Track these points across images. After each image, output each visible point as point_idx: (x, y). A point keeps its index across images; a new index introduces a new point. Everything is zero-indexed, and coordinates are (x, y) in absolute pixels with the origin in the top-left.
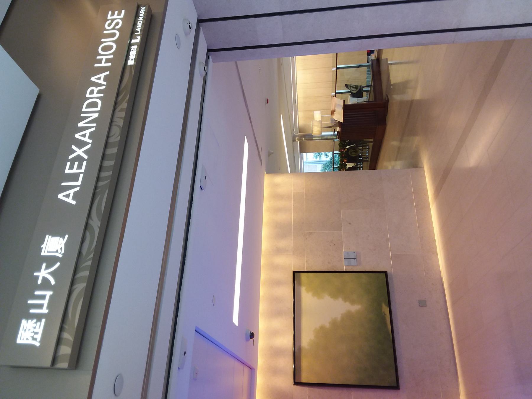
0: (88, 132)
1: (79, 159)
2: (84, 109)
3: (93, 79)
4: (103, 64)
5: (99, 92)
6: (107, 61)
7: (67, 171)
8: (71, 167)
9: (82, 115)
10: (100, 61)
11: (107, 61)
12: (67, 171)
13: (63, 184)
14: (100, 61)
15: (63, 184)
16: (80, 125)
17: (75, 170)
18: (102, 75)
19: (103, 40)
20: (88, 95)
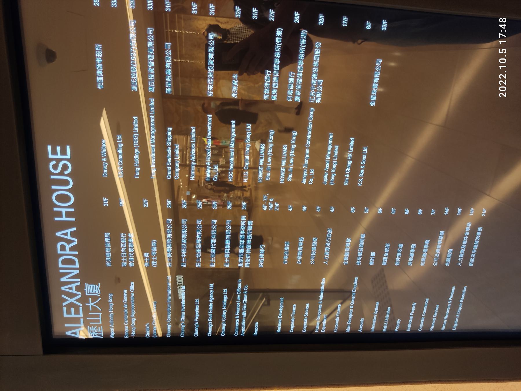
0: (73, 286)
1: (72, 305)
2: (61, 266)
3: (58, 234)
4: (64, 218)
5: (71, 249)
6: (68, 214)
7: (66, 315)
8: (69, 312)
9: (61, 271)
10: (59, 214)
11: (68, 214)
12: (66, 315)
13: (66, 325)
14: (59, 214)
15: (66, 325)
16: (63, 279)
17: (73, 315)
18: (69, 231)
19: (53, 187)
20: (59, 252)
